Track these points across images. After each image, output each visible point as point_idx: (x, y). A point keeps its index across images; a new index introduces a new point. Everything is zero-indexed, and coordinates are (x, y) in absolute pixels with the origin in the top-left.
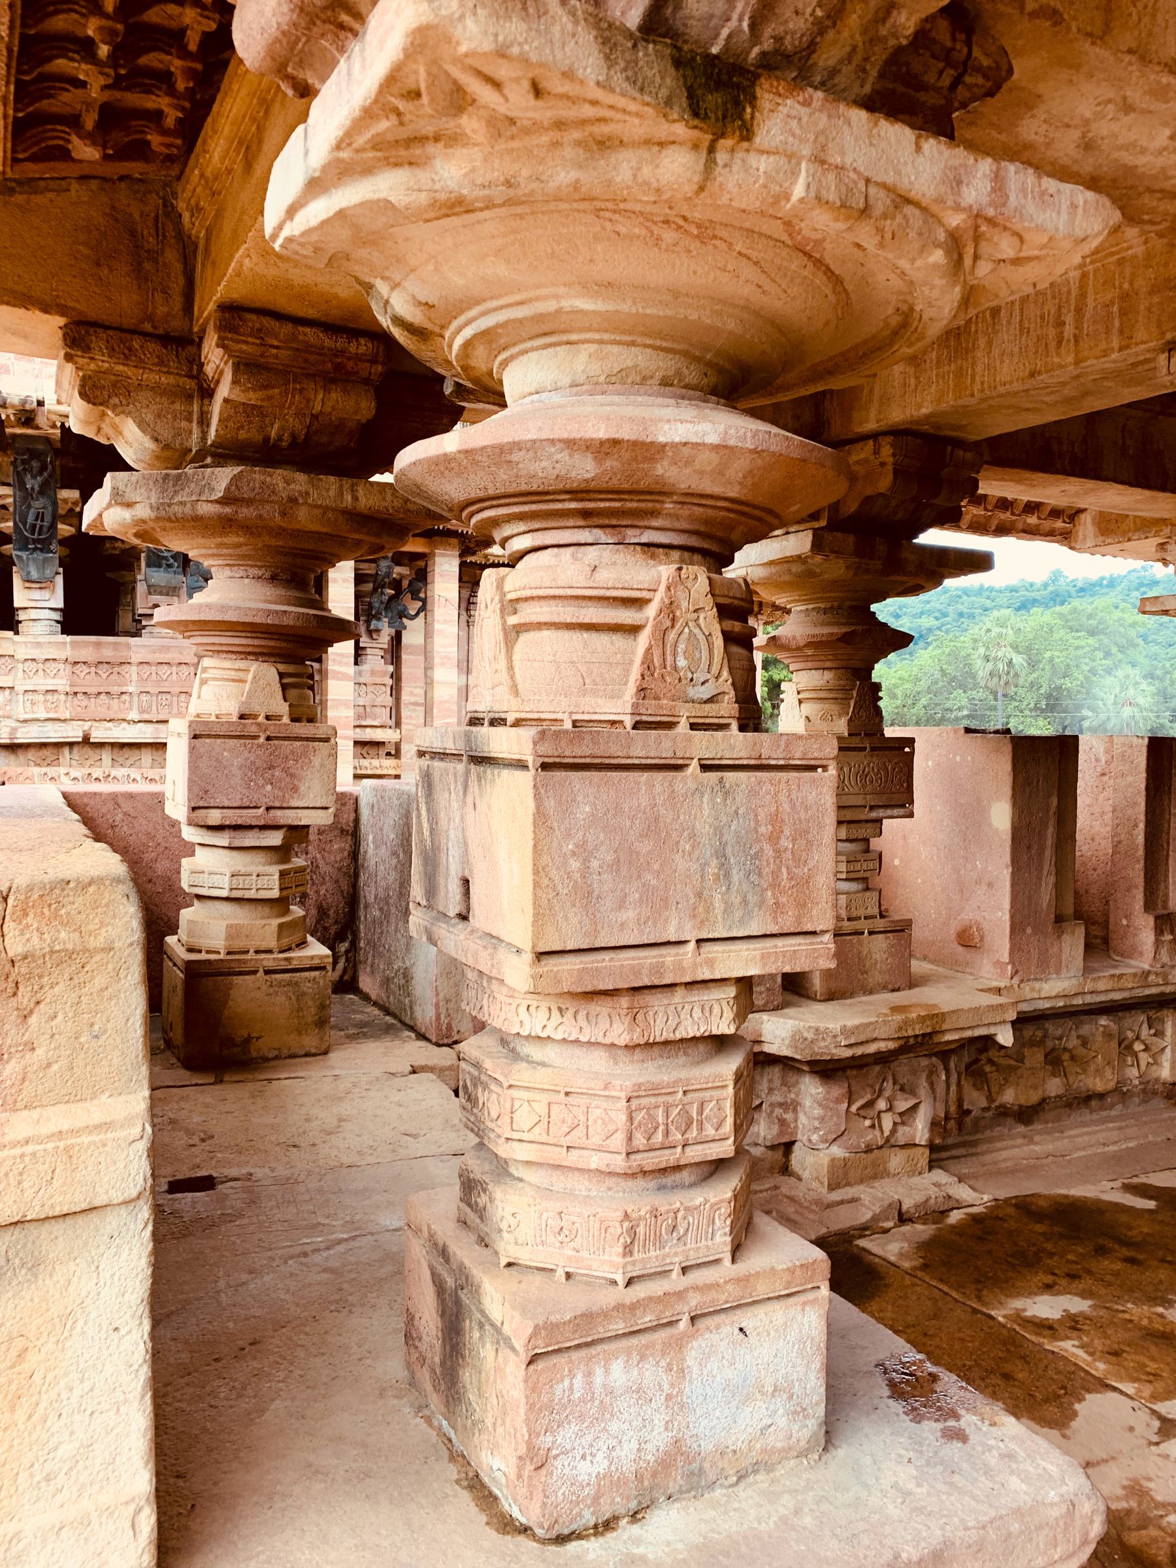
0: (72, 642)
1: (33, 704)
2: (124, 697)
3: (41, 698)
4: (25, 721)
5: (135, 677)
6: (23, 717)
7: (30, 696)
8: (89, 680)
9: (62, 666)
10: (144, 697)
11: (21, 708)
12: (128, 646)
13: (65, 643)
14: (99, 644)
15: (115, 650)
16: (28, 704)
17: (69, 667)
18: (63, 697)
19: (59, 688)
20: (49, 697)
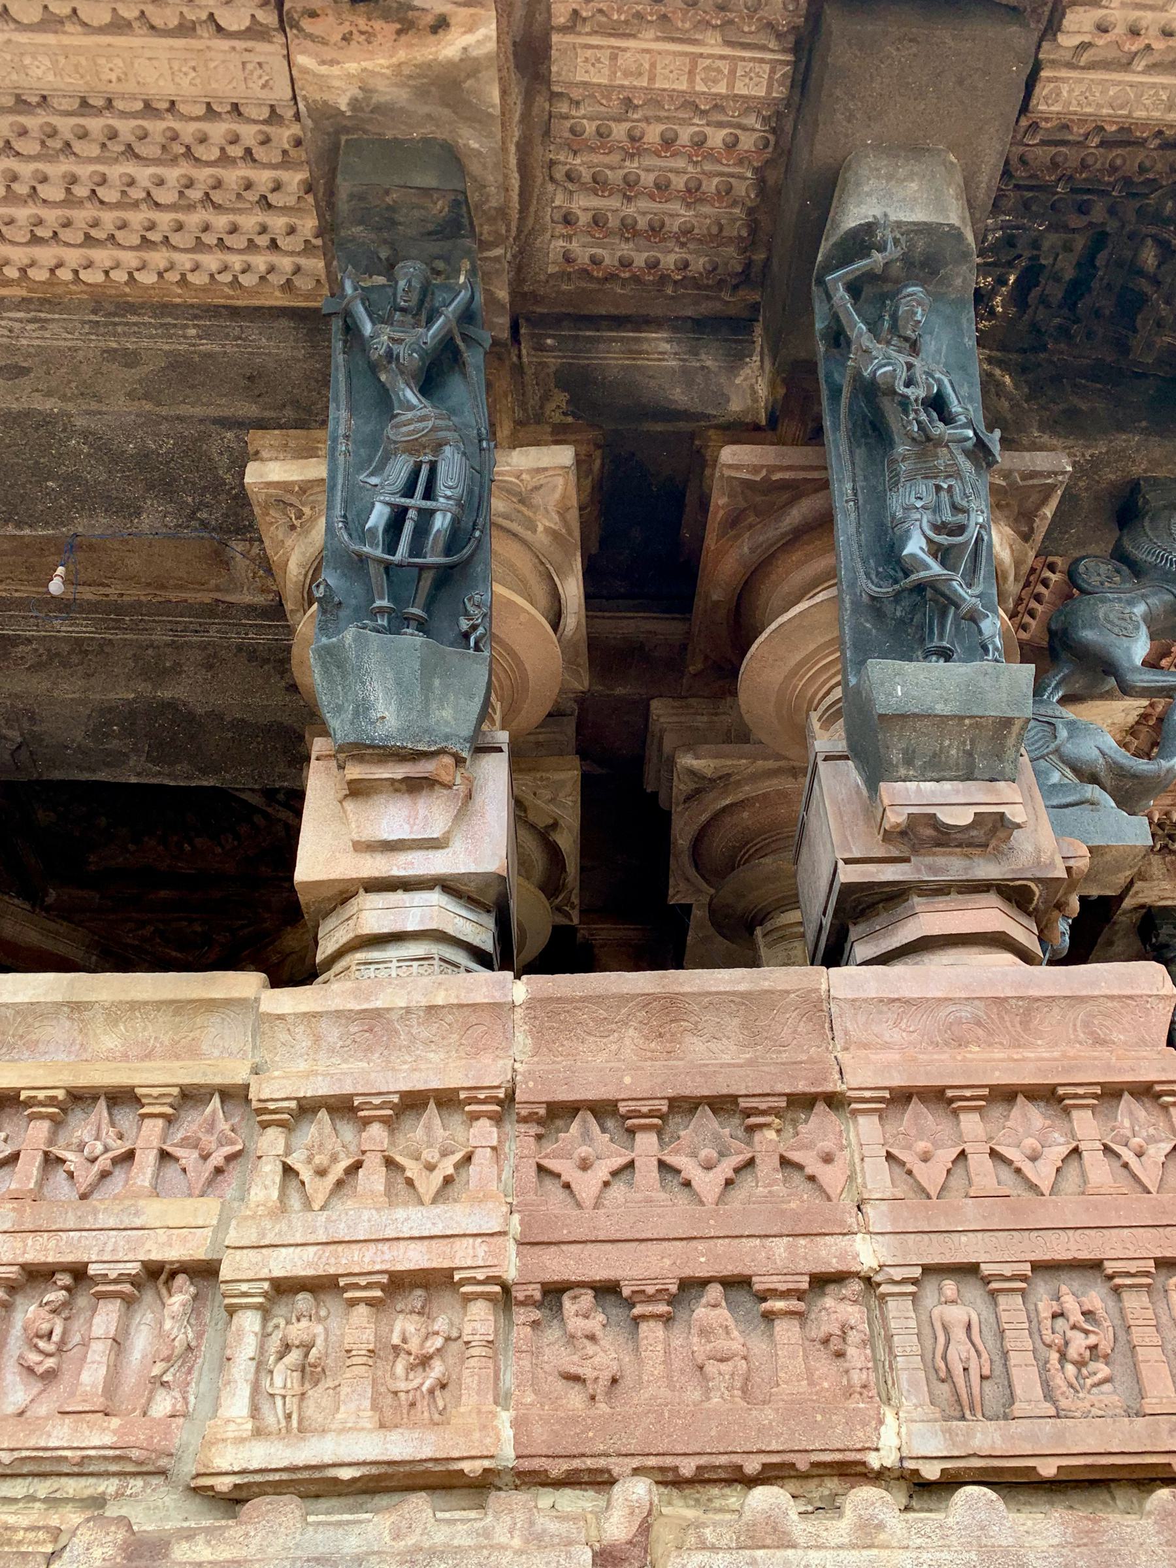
0: (532, 1004)
1: (310, 1373)
2: (839, 1309)
3: (358, 1327)
4: (234, 1501)
5: (878, 1179)
6: (237, 1457)
7: (302, 1323)
8: (637, 1216)
9: (484, 1132)
10: (958, 1308)
11: (236, 1405)
12: (819, 1011)
13: (500, 1010)
14: (671, 1006)
15: (753, 1035)
16: (282, 1377)
17: (520, 1142)
18: (480, 1319)
19: (465, 1256)
20: (405, 1326)
